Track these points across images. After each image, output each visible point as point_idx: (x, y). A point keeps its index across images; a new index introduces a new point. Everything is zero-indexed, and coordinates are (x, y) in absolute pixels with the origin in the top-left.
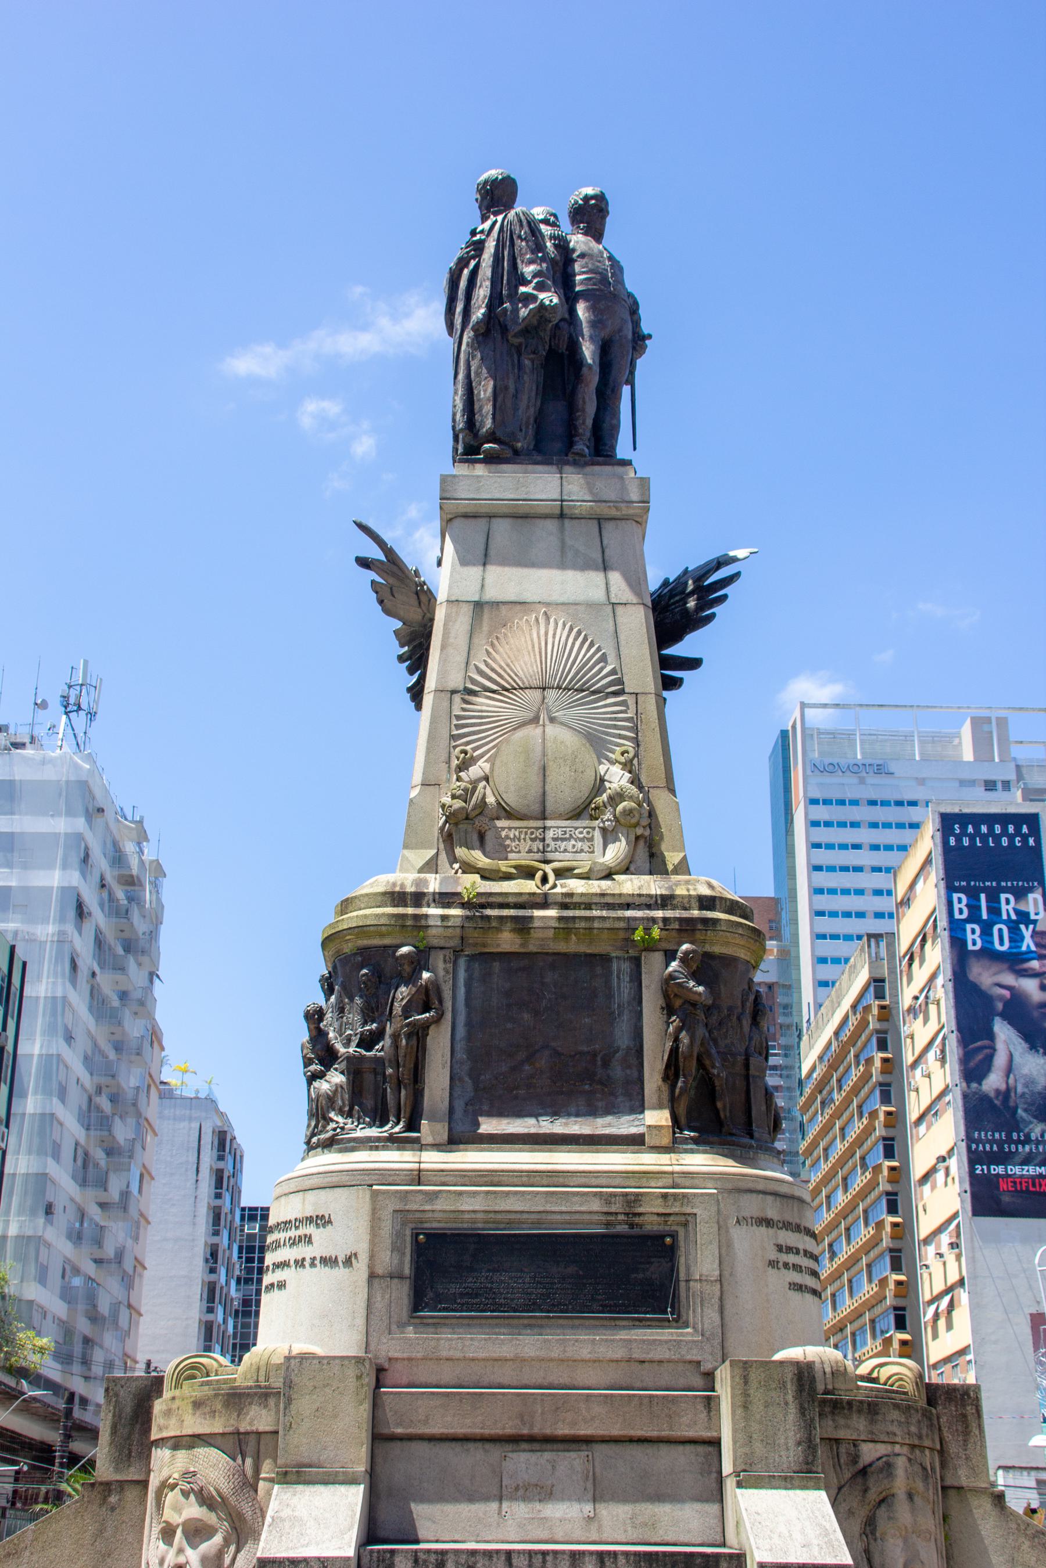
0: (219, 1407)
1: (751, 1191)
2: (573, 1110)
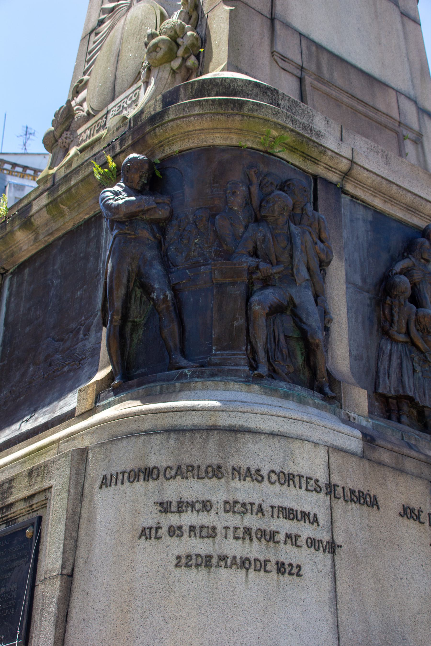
1: (129, 435)
2: (48, 400)
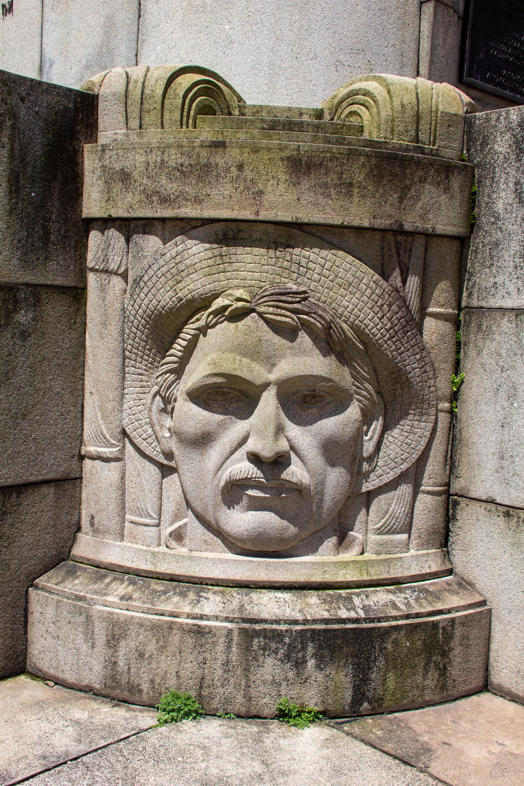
0: (359, 177)
